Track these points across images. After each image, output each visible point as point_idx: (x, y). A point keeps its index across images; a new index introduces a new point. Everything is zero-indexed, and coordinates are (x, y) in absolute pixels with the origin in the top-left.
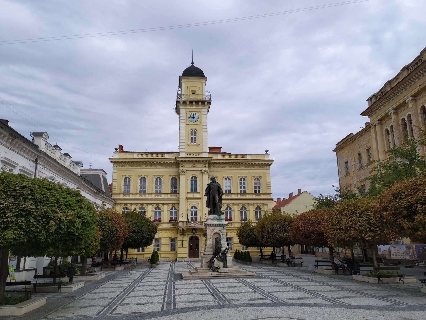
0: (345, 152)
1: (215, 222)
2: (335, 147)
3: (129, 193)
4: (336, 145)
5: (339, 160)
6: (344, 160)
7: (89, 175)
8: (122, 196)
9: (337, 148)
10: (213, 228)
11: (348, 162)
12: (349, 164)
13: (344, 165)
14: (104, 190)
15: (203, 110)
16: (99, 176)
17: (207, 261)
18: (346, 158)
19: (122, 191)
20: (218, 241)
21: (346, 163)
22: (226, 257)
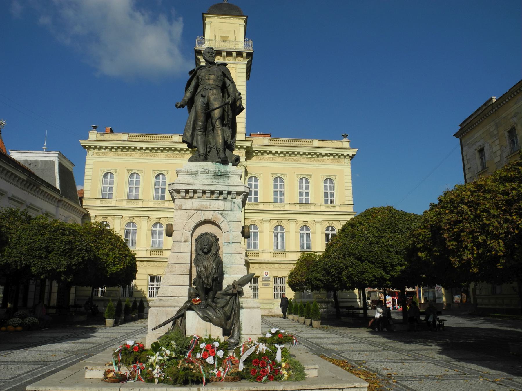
0: (478, 135)
1: (206, 182)
2: (457, 129)
3: (110, 198)
4: (460, 125)
5: (464, 149)
6: (477, 146)
7: (36, 161)
8: (98, 203)
9: (460, 130)
10: (196, 203)
11: (485, 149)
12: (487, 153)
13: (477, 155)
14: (58, 187)
15: (239, 66)
16: (52, 162)
17: (164, 320)
18: (480, 143)
19: (99, 195)
20: (207, 247)
21: (481, 151)
22: (237, 308)
